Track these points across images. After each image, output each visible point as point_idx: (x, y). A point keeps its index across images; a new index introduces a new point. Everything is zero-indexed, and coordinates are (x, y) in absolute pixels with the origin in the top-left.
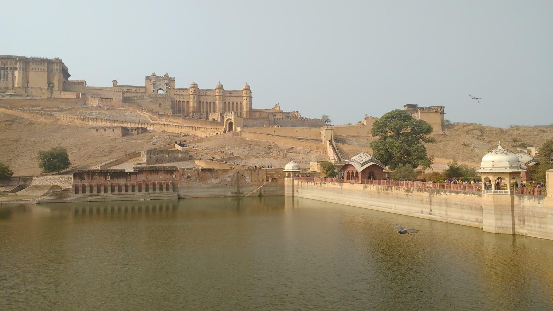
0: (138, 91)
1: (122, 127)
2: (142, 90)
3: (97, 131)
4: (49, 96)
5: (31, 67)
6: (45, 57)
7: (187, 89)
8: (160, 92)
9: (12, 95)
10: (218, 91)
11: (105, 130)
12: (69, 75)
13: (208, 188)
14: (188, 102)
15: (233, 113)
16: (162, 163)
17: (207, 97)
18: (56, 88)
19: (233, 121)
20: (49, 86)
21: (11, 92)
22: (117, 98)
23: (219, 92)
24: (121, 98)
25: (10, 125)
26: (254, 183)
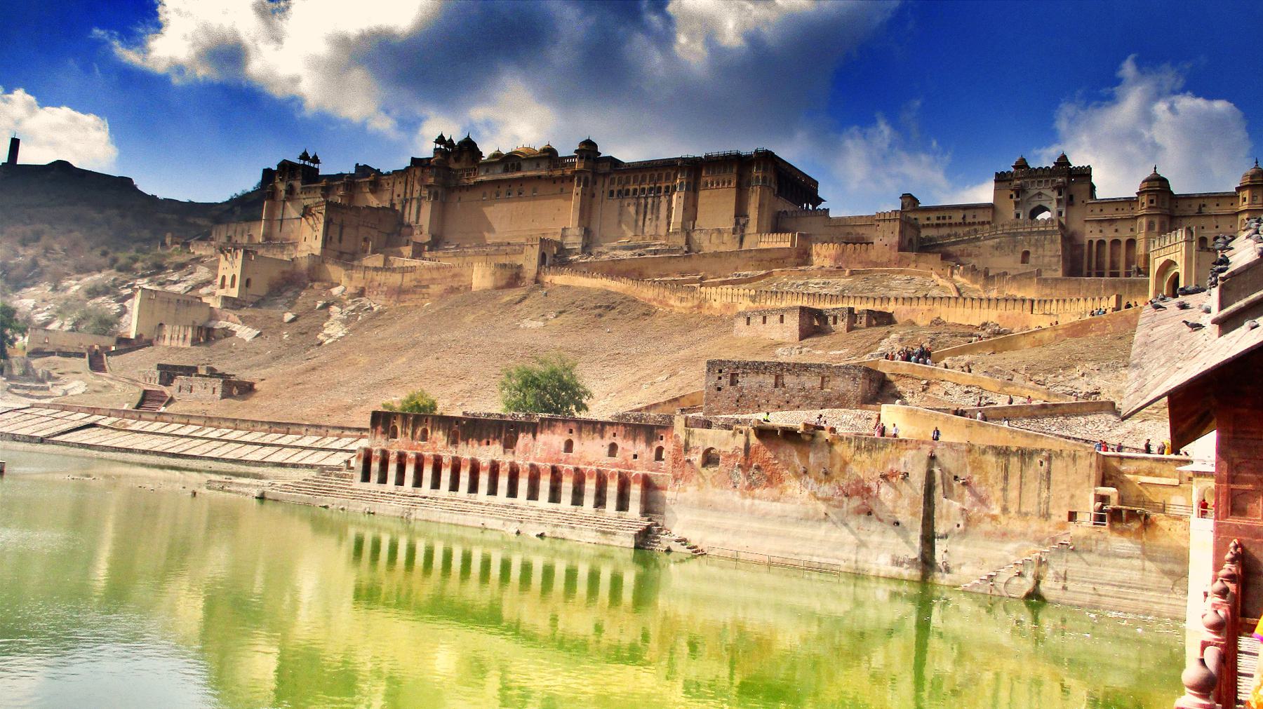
0: (969, 220)
1: (802, 309)
2: (983, 216)
3: (748, 324)
4: (736, 248)
5: (703, 180)
6: (734, 152)
7: (1129, 201)
8: (1045, 215)
9: (656, 252)
10: (1246, 194)
11: (765, 318)
12: (820, 201)
13: (783, 518)
14: (1131, 243)
15: (1181, 235)
16: (759, 408)
17: (1203, 222)
18: (752, 227)
19: (1180, 269)
20: (737, 223)
21: (659, 244)
22: (885, 241)
23: (1253, 198)
24: (896, 238)
25: (600, 316)
26: (1017, 526)
